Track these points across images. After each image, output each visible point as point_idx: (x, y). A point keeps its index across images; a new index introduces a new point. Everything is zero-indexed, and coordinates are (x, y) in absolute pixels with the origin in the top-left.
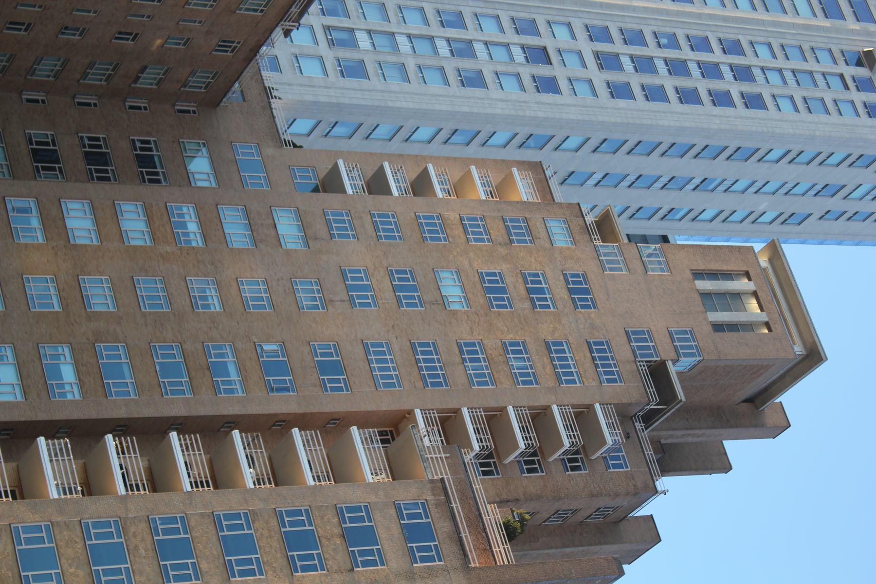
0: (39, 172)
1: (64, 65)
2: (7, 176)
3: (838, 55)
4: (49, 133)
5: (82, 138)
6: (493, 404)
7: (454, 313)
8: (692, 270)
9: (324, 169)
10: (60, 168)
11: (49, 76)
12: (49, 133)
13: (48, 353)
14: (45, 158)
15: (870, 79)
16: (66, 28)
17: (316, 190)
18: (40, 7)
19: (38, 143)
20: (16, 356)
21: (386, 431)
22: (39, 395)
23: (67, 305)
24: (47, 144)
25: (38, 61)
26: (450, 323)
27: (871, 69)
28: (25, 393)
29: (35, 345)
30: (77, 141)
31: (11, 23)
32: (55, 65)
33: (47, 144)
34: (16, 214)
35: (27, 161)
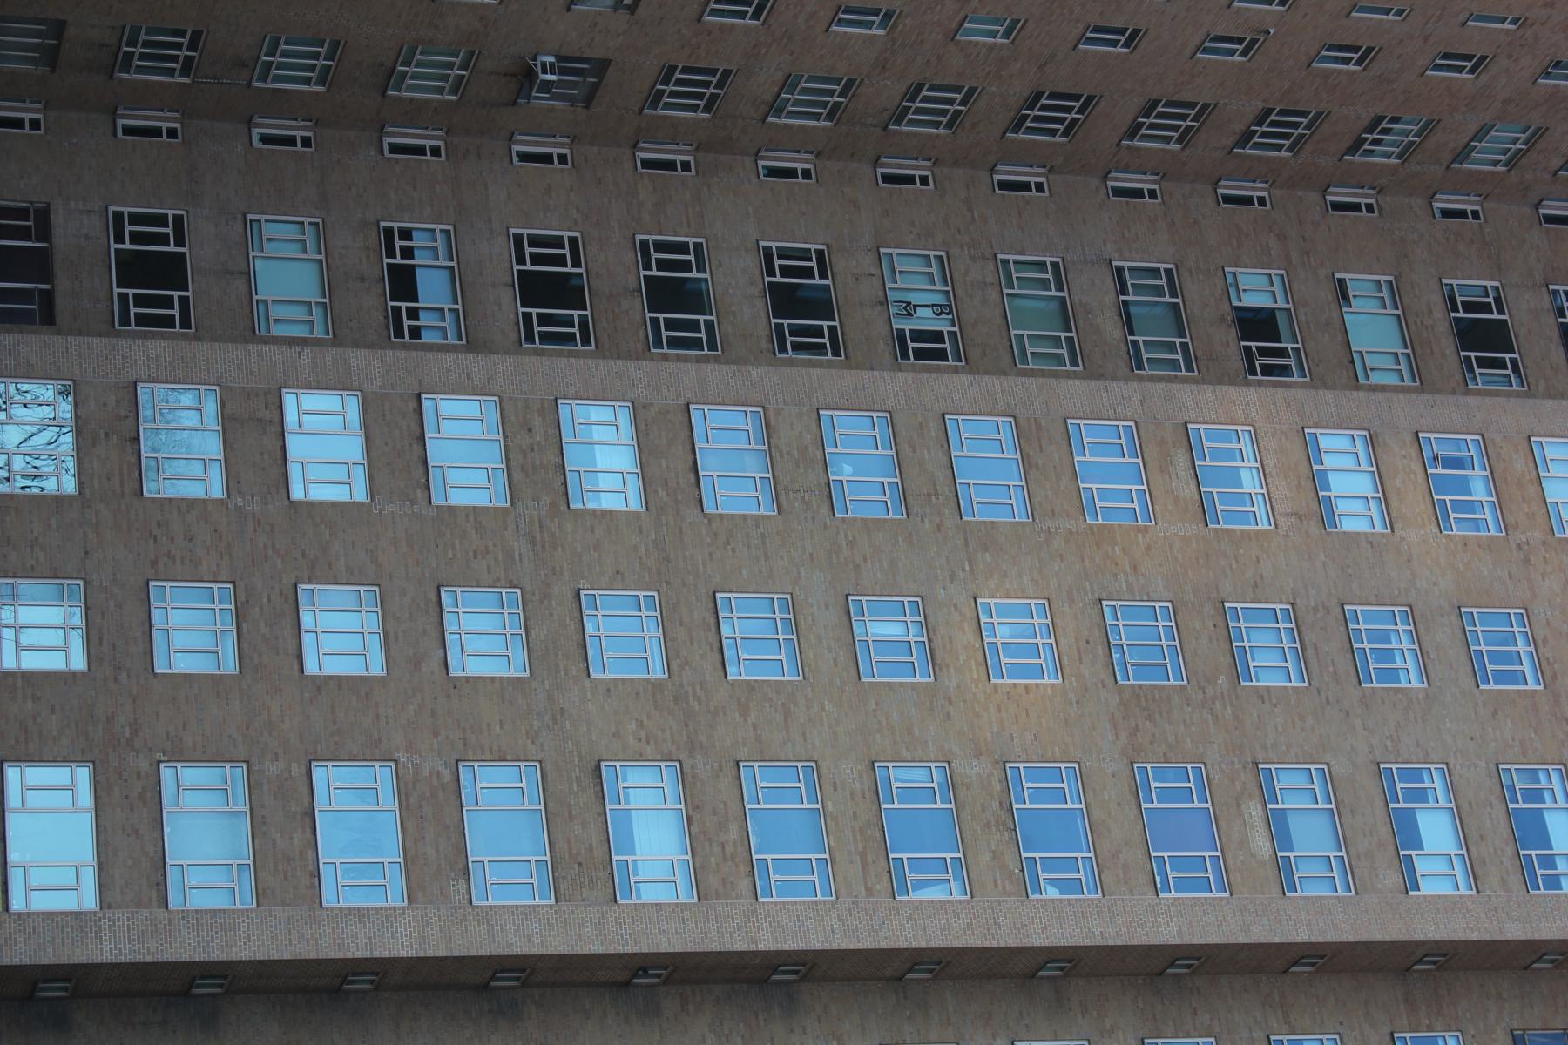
0: (1471, 370)
1: (1531, 142)
2: (1408, 382)
4: (1489, 284)
5: (1556, 292)
10: (1514, 363)
11: (1495, 163)
12: (1489, 284)
13: (1518, 786)
14: (1483, 337)
16: (1557, 65)
18: (1515, 21)
19: (1468, 307)
20: (1453, 791)
22: (1504, 882)
23: (1554, 677)
24: (1485, 308)
25: (1481, 133)
28: (1476, 879)
29: (1493, 767)
30: (1546, 301)
31: (1446, 56)
32: (1515, 141)
33: (1485, 308)
34: (1440, 471)
35: (1446, 343)
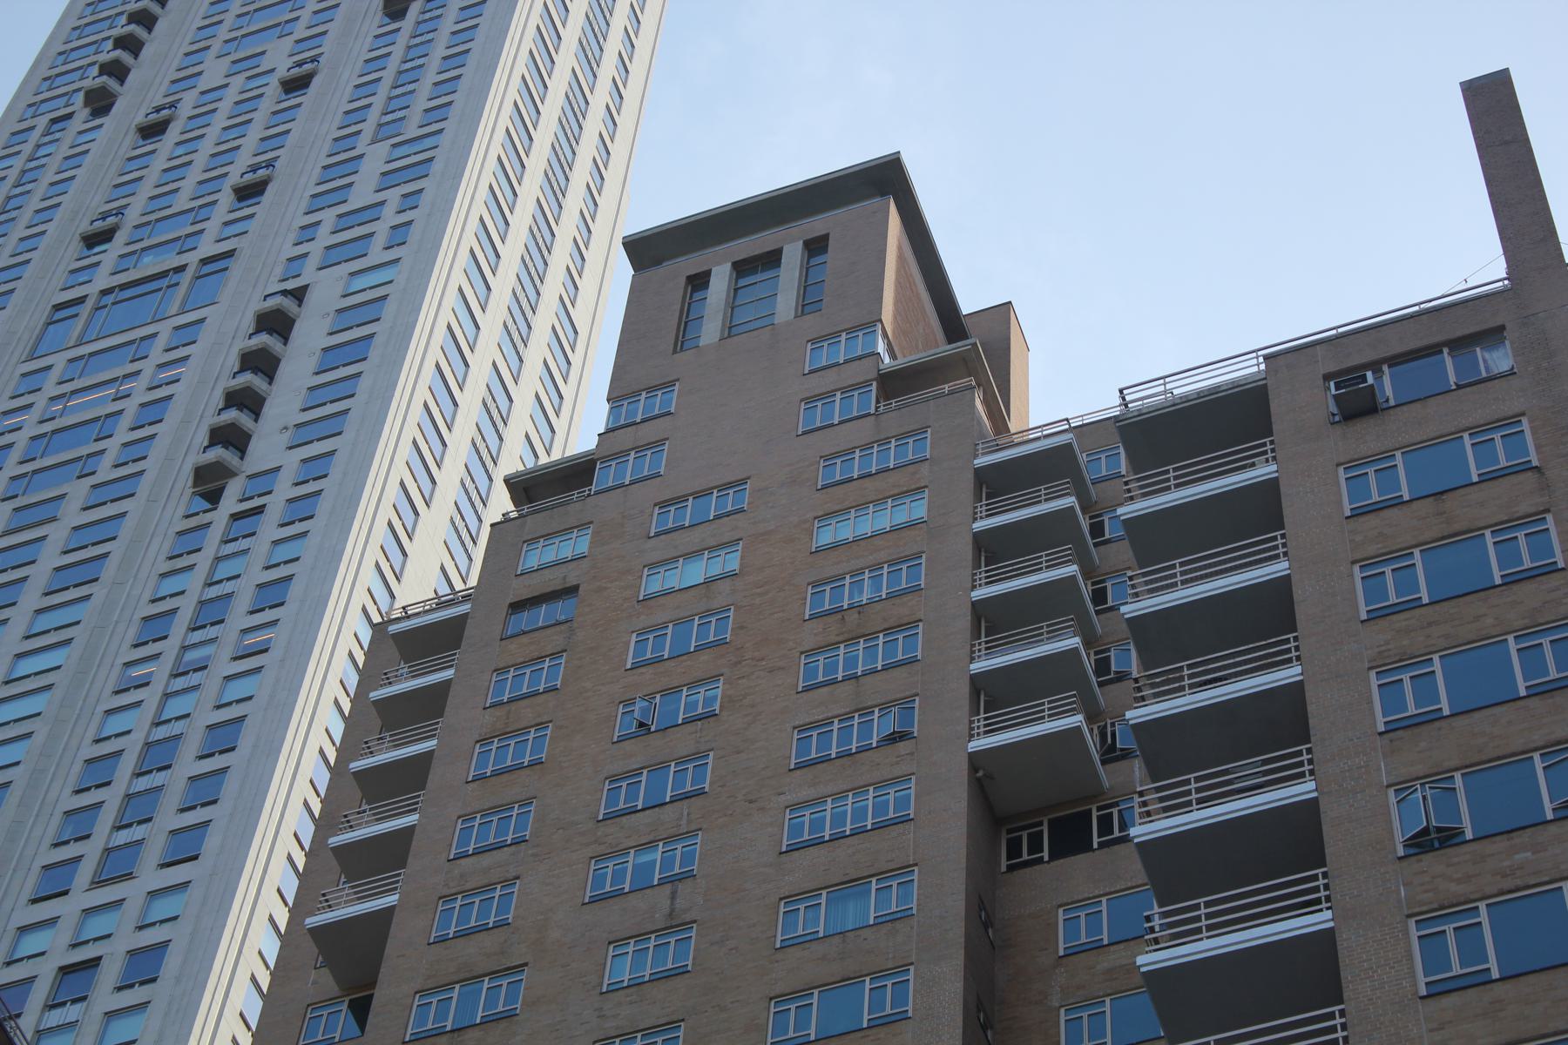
3: (193, 522)
6: (964, 622)
7: (728, 702)
8: (675, 352)
9: (323, 982)
15: (250, 477)
17: (361, 1010)
21: (1009, 841)
26: (753, 706)
27: (231, 474)
